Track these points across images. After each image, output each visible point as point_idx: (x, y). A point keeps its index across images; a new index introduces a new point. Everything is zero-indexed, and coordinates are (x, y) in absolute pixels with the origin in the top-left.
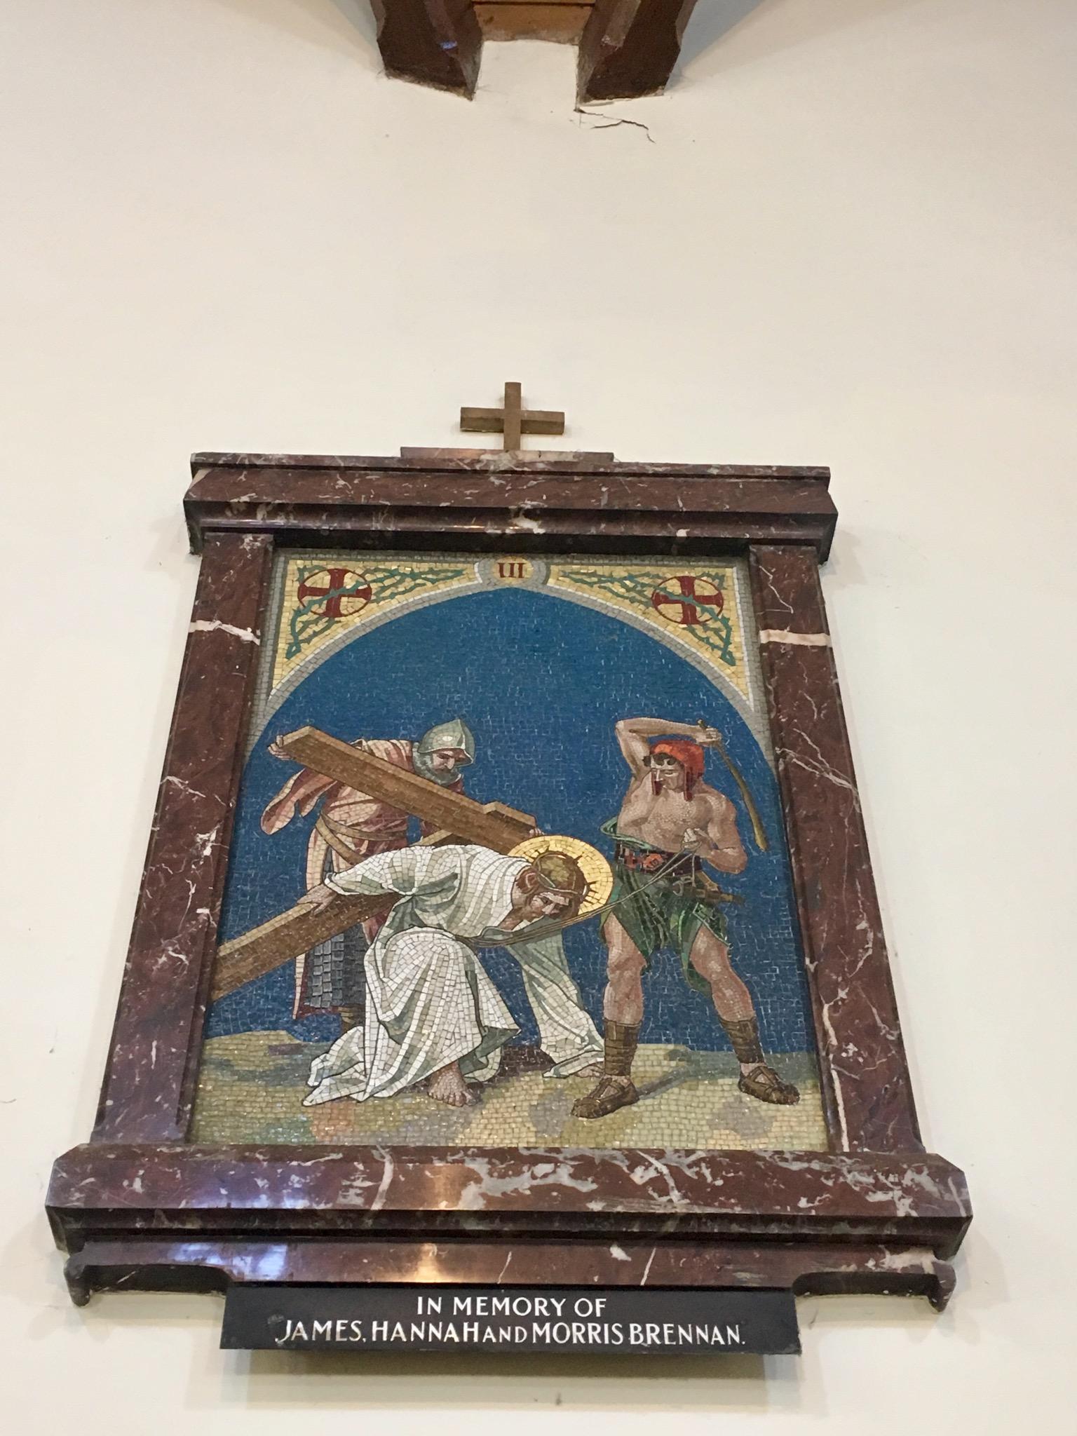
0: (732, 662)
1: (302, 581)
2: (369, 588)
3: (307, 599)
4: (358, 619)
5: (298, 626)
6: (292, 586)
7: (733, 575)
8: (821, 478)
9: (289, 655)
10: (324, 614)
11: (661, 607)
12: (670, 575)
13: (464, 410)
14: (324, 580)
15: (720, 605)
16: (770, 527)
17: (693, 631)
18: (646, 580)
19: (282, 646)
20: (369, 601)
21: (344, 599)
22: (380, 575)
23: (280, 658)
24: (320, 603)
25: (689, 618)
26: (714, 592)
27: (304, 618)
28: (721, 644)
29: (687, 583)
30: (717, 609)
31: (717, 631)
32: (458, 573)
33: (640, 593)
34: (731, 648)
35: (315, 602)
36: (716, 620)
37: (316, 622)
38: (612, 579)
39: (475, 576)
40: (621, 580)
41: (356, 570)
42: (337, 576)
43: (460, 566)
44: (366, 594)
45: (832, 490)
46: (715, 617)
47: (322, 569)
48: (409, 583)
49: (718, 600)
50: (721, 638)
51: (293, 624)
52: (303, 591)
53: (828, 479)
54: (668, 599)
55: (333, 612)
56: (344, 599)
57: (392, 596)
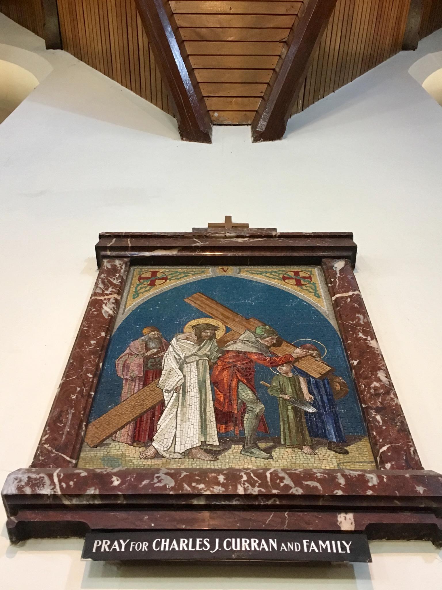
0: (319, 297)
2: (167, 277)
3: (142, 281)
7: (316, 271)
8: (350, 236)
12: (290, 270)
13: (209, 224)
14: (149, 275)
17: (302, 288)
18: (280, 272)
21: (157, 281)
25: (298, 283)
29: (297, 273)
32: (203, 272)
33: (278, 276)
36: (310, 284)
37: (146, 288)
38: (266, 273)
41: (162, 270)
42: (154, 274)
43: (204, 270)
45: (355, 240)
46: (310, 283)
49: (310, 278)
50: (313, 289)
51: (136, 288)
52: (140, 278)
53: (353, 236)
54: (290, 278)
55: (153, 284)
56: (157, 281)
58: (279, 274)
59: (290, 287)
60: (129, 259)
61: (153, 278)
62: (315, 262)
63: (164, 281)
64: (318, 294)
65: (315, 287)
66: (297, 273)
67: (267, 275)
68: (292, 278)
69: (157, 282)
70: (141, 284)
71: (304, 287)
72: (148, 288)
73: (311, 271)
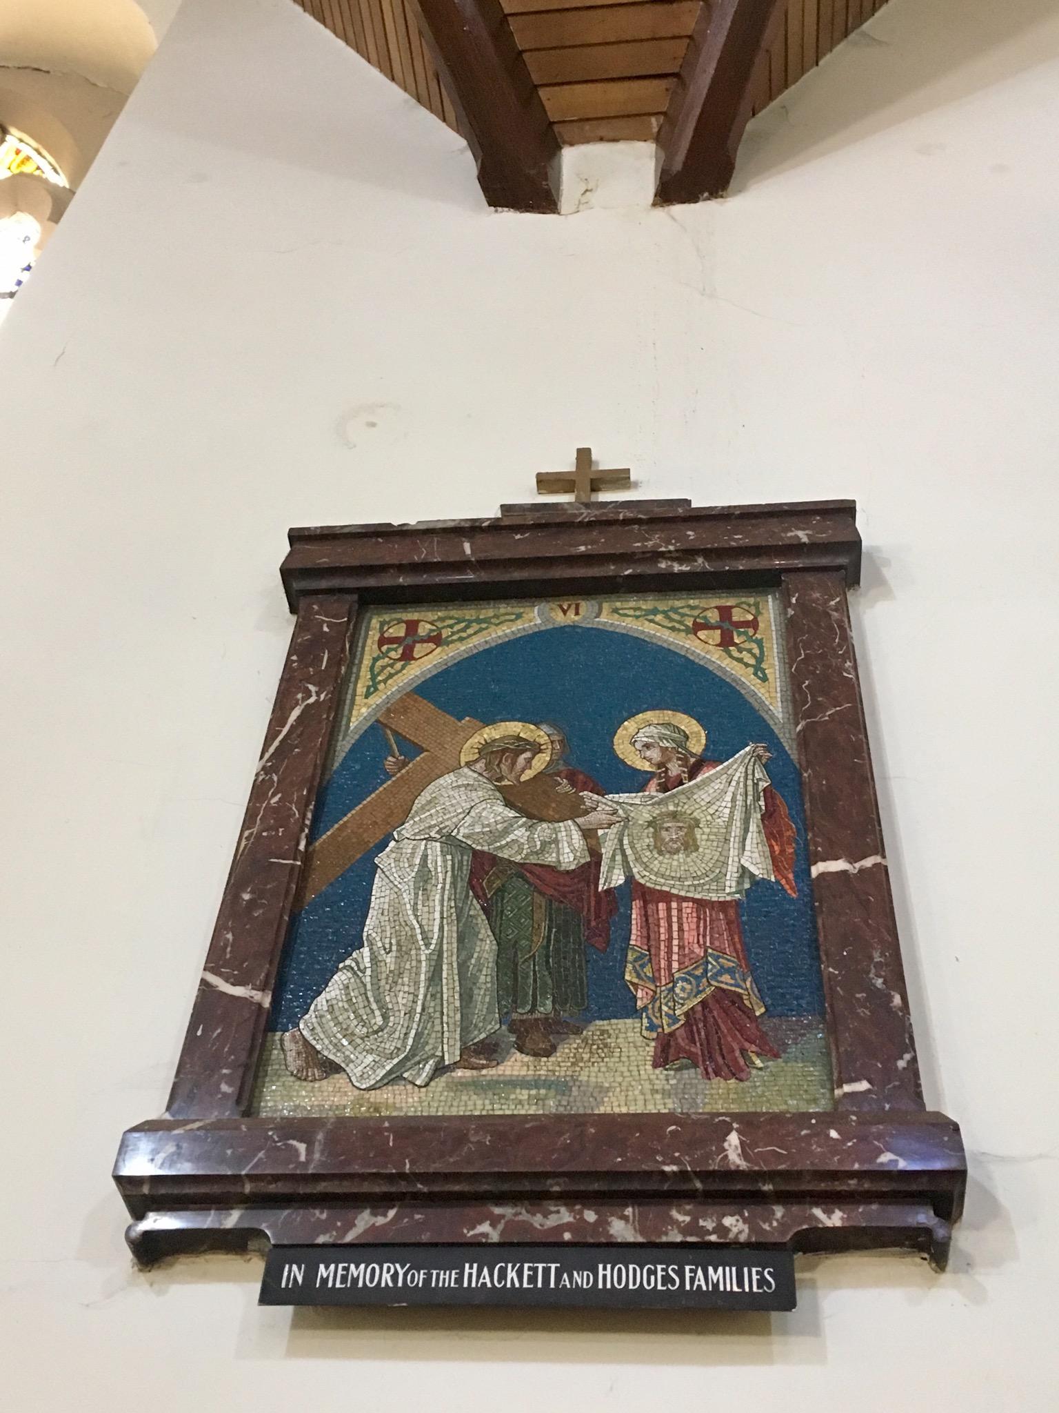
0: (764, 679)
1: (382, 633)
2: (440, 635)
3: (384, 648)
4: (429, 661)
5: (376, 670)
6: (374, 635)
8: (844, 511)
12: (709, 605)
14: (399, 631)
15: (756, 628)
19: (361, 689)
21: (418, 646)
22: (451, 622)
24: (395, 650)
25: (726, 642)
26: (750, 617)
27: (379, 663)
28: (752, 661)
29: (725, 612)
30: (751, 631)
31: (749, 651)
32: (519, 616)
34: (764, 666)
37: (392, 666)
39: (534, 618)
41: (427, 619)
42: (412, 626)
43: (517, 610)
44: (437, 640)
46: (750, 639)
47: (400, 621)
48: (475, 627)
49: (754, 624)
50: (754, 655)
51: (372, 668)
52: (382, 641)
54: (707, 626)
55: (408, 657)
56: (418, 646)
58: (683, 615)
60: (355, 597)
61: (409, 640)
63: (432, 646)
64: (763, 671)
66: (725, 612)
67: (659, 618)
69: (419, 650)
70: (385, 655)
72: (399, 665)
73: (756, 605)
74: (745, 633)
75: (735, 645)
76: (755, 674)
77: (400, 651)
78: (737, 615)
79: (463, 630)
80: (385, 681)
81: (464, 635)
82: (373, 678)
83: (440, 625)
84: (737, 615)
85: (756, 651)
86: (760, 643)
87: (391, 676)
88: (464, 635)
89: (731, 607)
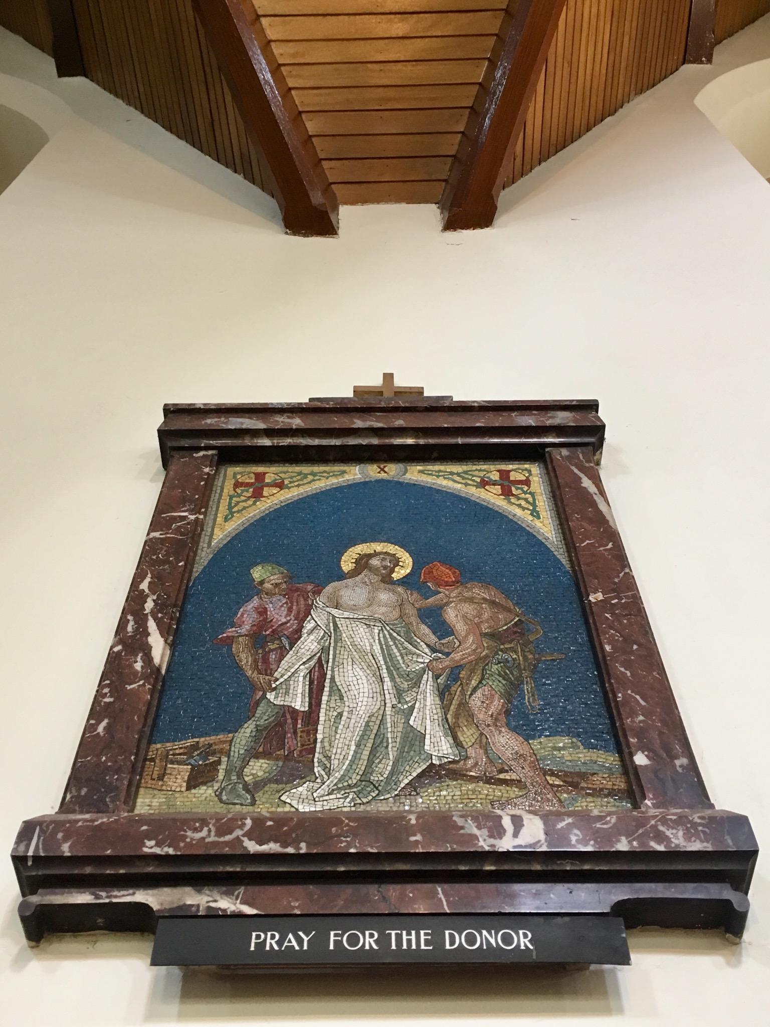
2: (283, 482)
4: (274, 499)
7: (535, 469)
9: (226, 519)
10: (251, 497)
11: (487, 487)
12: (492, 471)
16: (560, 438)
18: (476, 473)
20: (281, 489)
23: (220, 520)
24: (247, 491)
25: (507, 493)
26: (524, 478)
29: (504, 475)
30: (526, 488)
35: (243, 491)
39: (354, 473)
40: (458, 474)
41: (272, 472)
42: (260, 477)
44: (280, 485)
46: (525, 493)
49: (527, 482)
50: (528, 502)
52: (237, 485)
55: (258, 495)
57: (298, 486)
59: (492, 497)
62: (535, 454)
64: (538, 512)
65: (534, 500)
66: (504, 475)
68: (494, 484)
69: (266, 491)
70: (239, 496)
71: (513, 500)
72: (250, 502)
74: (522, 489)
75: (513, 495)
76: (532, 514)
77: (251, 490)
78: (514, 476)
79: (301, 480)
80: (238, 512)
81: (301, 483)
82: (230, 508)
83: (282, 475)
84: (514, 476)
85: (531, 500)
86: (532, 494)
87: (245, 508)
88: (301, 483)
89: (510, 471)
